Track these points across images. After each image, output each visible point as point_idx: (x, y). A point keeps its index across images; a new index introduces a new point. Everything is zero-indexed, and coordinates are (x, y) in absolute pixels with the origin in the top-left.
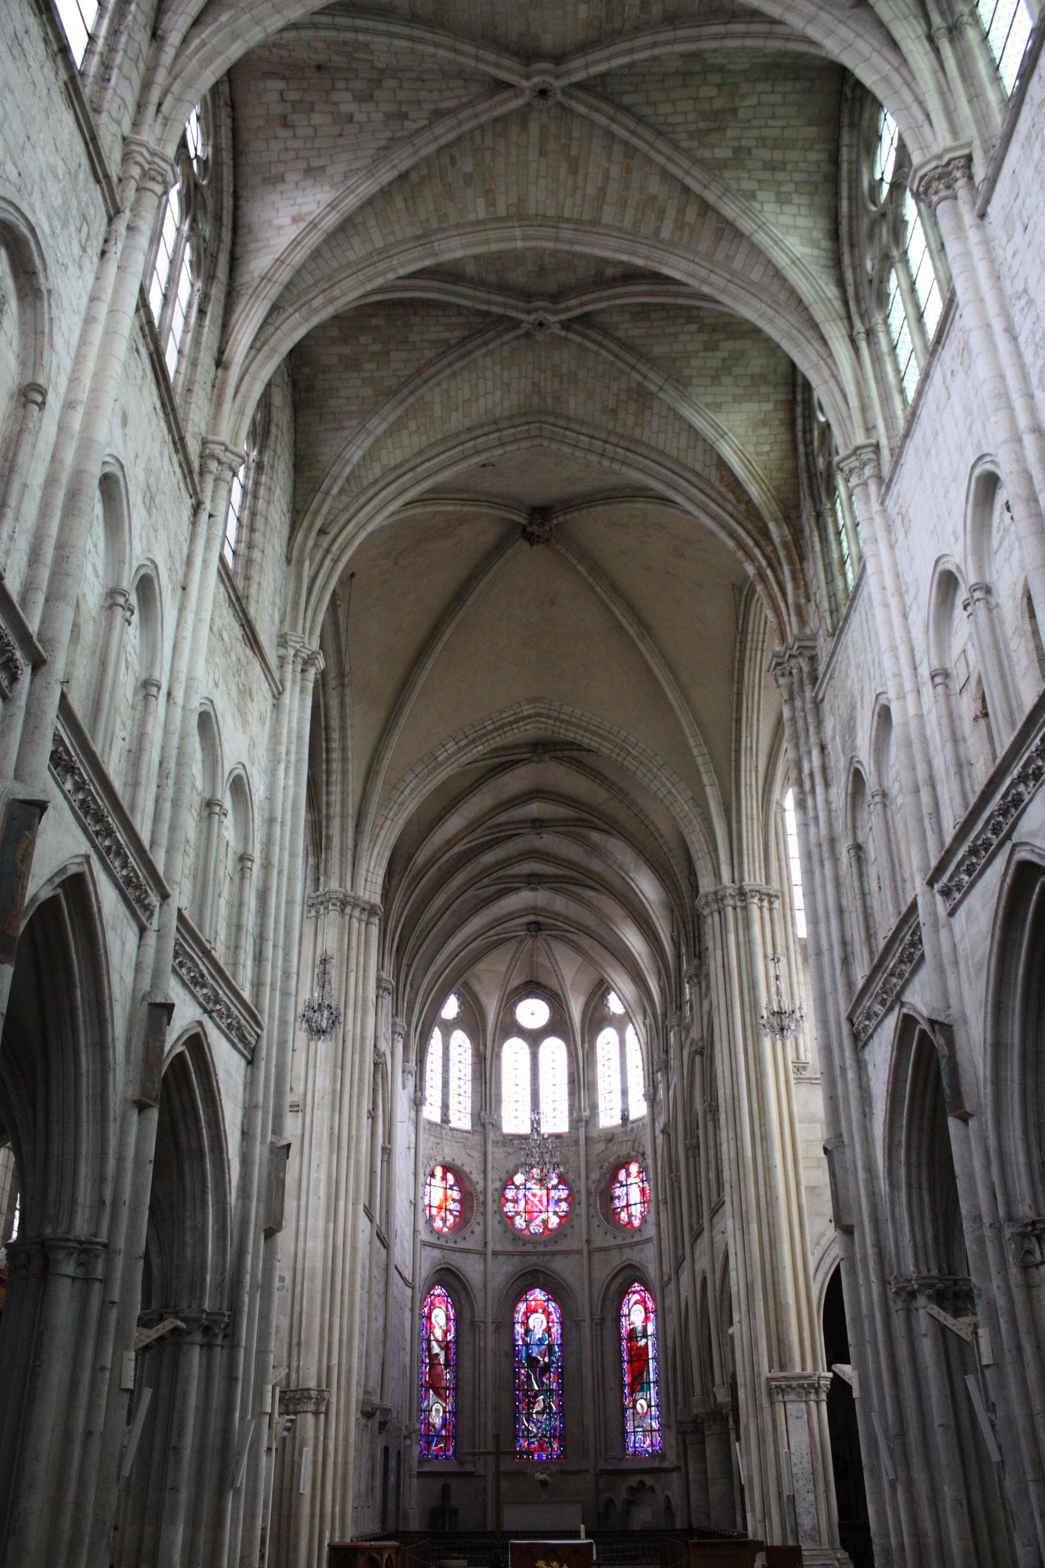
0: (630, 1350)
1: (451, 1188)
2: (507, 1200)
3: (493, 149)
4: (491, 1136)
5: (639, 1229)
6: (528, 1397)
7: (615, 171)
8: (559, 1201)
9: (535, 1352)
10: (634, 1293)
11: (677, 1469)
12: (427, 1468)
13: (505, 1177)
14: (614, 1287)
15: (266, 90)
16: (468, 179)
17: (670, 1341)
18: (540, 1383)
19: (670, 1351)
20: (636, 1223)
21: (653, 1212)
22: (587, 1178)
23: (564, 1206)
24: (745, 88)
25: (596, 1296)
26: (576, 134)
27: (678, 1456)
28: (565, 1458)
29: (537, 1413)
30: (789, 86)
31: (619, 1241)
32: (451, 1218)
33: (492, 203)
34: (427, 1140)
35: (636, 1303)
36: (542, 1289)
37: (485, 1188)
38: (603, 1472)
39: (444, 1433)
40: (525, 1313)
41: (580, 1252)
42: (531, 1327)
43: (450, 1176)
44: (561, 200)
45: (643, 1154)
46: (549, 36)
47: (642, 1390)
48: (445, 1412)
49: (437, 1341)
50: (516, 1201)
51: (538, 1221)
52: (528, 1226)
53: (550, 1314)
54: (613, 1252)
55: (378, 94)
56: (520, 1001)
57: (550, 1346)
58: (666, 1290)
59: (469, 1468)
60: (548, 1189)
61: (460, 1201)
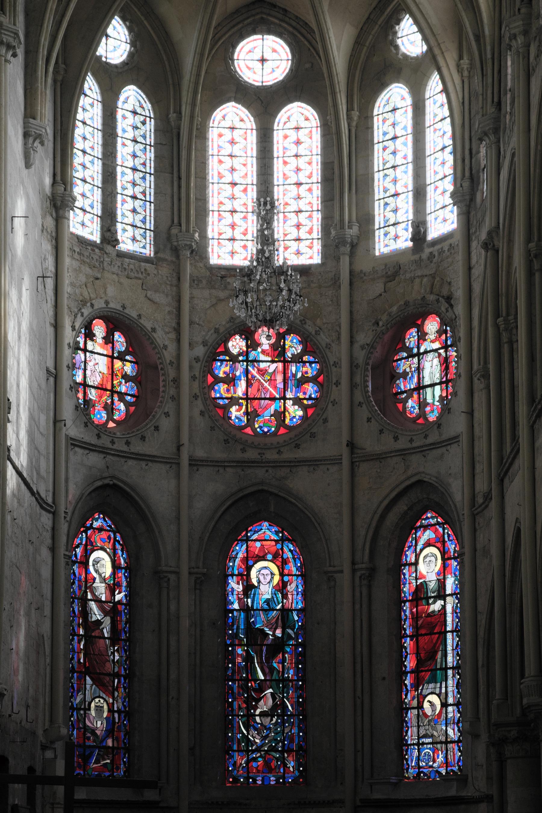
0: (416, 617)
1: (121, 357)
2: (218, 380)
4: (188, 269)
5: (438, 424)
6: (248, 690)
8: (304, 380)
10: (426, 527)
13: (211, 337)
14: (392, 518)
17: (483, 604)
18: (269, 670)
19: (482, 620)
20: (432, 417)
22: (352, 342)
23: (311, 389)
31: (402, 443)
32: (122, 407)
34: (78, 271)
36: (272, 522)
37: (178, 357)
39: (110, 743)
41: (337, 461)
42: (254, 581)
43: (117, 336)
47: (434, 680)
48: (111, 710)
49: (98, 601)
50: (231, 380)
51: (267, 415)
52: (250, 423)
53: (285, 562)
56: (242, 37)
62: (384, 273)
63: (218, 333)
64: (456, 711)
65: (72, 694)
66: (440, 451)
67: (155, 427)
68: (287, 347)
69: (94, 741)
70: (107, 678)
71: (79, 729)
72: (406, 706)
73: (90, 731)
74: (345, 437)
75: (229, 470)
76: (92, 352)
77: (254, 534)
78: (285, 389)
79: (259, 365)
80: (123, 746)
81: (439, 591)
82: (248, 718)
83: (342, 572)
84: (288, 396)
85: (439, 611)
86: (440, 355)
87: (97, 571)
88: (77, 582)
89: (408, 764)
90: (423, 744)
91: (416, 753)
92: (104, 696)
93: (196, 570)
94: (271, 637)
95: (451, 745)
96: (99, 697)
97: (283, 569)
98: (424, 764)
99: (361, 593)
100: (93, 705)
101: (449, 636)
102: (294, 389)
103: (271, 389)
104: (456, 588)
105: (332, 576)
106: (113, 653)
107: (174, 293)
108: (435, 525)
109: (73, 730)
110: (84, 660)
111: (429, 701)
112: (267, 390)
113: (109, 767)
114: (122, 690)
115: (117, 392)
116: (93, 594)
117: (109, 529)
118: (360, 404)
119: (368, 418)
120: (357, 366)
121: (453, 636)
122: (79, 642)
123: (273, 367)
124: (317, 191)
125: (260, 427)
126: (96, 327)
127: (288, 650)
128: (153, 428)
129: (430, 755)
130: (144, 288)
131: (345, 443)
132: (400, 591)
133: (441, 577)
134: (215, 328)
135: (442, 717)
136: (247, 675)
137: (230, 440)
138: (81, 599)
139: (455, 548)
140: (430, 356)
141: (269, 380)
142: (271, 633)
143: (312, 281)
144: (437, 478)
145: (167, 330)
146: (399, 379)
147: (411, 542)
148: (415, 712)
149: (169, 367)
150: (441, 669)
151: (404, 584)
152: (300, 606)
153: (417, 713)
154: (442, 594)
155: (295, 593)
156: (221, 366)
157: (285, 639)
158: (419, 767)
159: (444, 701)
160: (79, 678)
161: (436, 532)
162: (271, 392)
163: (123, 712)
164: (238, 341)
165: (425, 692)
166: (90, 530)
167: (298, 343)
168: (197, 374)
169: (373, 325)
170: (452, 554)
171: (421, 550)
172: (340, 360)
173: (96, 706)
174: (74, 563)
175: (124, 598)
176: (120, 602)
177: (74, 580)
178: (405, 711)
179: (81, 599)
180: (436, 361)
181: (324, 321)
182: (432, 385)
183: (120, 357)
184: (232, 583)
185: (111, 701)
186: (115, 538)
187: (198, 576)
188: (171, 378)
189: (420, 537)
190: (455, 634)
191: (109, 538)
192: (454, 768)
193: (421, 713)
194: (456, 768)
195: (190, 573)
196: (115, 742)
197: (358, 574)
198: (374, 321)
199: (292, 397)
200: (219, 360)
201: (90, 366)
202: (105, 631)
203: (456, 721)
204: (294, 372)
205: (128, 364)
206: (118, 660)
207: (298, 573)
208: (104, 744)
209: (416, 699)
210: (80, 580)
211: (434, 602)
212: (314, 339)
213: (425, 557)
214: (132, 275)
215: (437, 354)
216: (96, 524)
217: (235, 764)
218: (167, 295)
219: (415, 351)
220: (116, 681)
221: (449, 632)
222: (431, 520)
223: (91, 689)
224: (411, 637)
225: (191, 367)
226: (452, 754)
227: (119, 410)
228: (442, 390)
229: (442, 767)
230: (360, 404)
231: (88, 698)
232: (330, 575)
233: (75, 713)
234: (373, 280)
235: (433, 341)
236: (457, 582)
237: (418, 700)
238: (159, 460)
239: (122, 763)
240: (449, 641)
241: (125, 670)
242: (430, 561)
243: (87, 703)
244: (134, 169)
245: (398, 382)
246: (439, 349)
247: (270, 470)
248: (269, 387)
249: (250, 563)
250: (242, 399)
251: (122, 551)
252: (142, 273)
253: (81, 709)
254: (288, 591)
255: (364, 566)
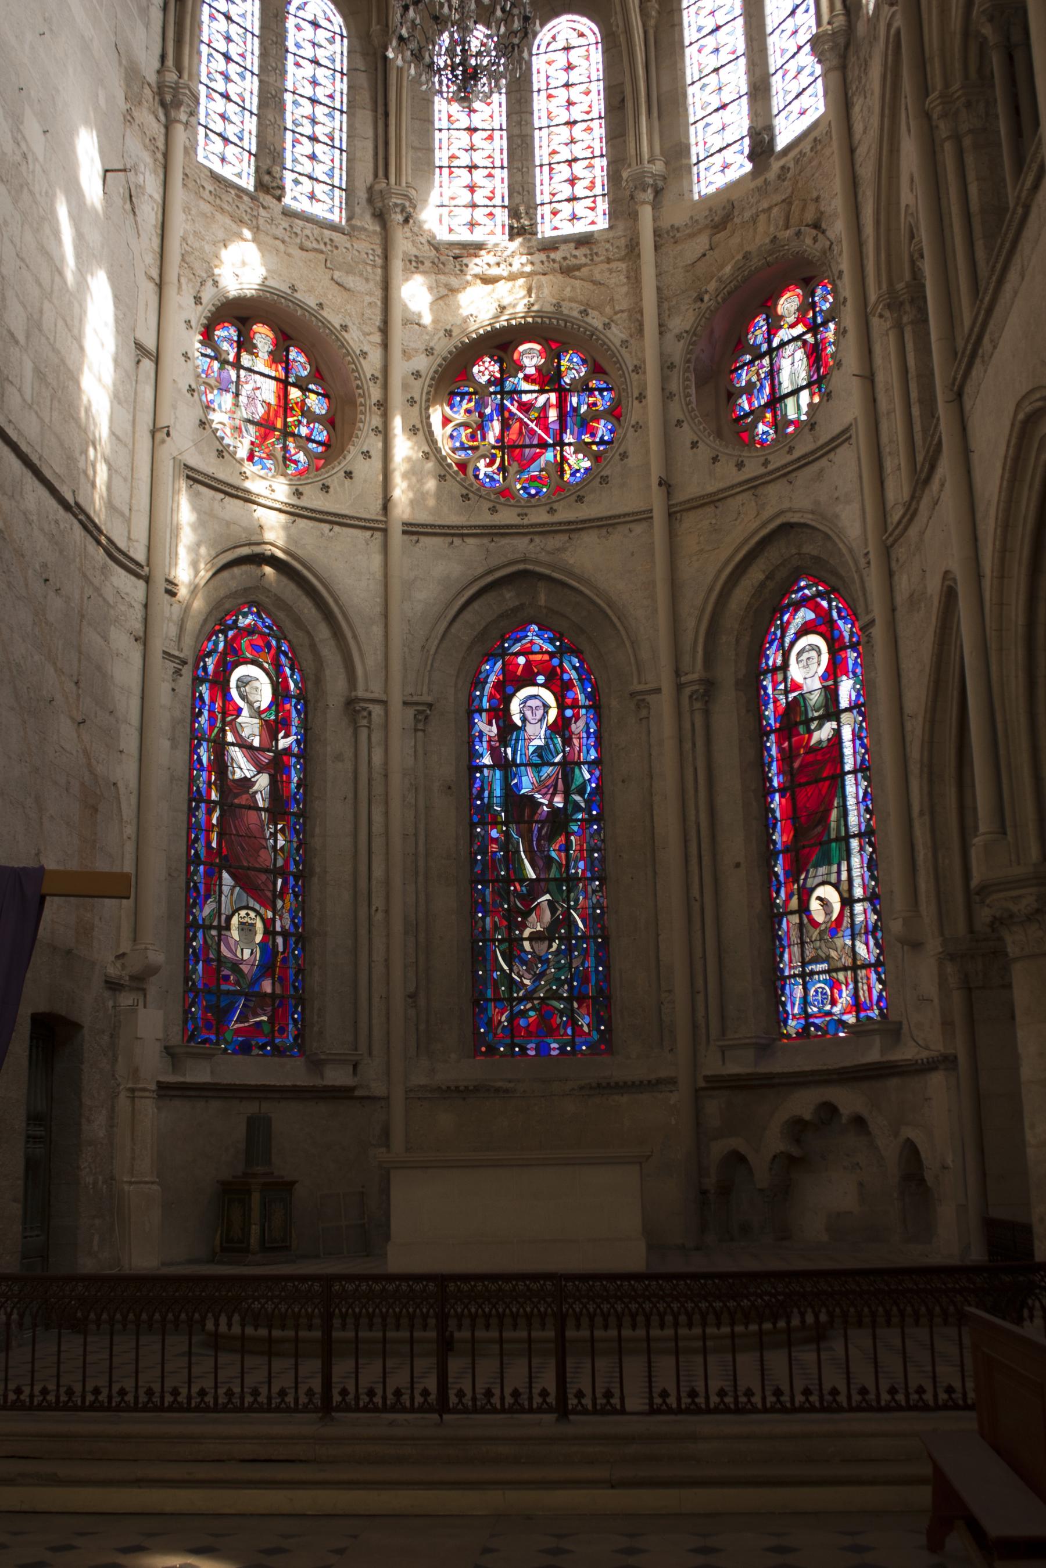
0: (786, 758)
4: (403, 244)
9: (527, 782)
10: (797, 606)
11: (947, 1062)
12: (199, 1074)
14: (741, 595)
18: (542, 862)
21: (851, 338)
22: (662, 329)
23: (602, 429)
25: (690, 623)
27: (947, 1024)
28: (610, 1050)
29: (534, 938)
31: (753, 470)
32: (301, 457)
35: (806, 629)
38: (718, 1083)
39: (267, 986)
40: (498, 686)
41: (644, 517)
42: (517, 719)
45: (816, 226)
48: (269, 931)
49: (245, 746)
54: (734, 503)
57: (568, 767)
58: (900, 552)
59: (337, 1076)
60: (563, 394)
61: (330, 421)
62: (708, 222)
63: (450, 336)
64: (869, 911)
65: (195, 901)
66: (815, 467)
67: (345, 472)
68: (563, 369)
69: (237, 983)
70: (264, 877)
71: (207, 961)
72: (778, 910)
73: (229, 965)
74: (656, 471)
75: (470, 541)
76: (249, 370)
77: (514, 644)
78: (563, 428)
79: (520, 398)
80: (292, 992)
81: (826, 706)
82: (510, 945)
83: (658, 691)
84: (567, 441)
85: (828, 740)
86: (805, 342)
87: (243, 697)
88: (206, 713)
89: (786, 1012)
90: (812, 973)
91: (799, 992)
92: (257, 907)
93: (415, 699)
94: (545, 808)
95: (864, 972)
96: (247, 907)
97: (564, 696)
98: (815, 1009)
99: (693, 725)
100: (235, 921)
101: (850, 780)
102: (576, 429)
103: (540, 432)
104: (858, 696)
105: (643, 700)
106: (274, 835)
107: (378, 278)
108: (813, 597)
109: (197, 963)
110: (219, 843)
111: (819, 898)
112: (532, 432)
113: (266, 1029)
114: (290, 897)
115: (293, 434)
116: (236, 733)
117: (267, 631)
118: (679, 423)
119: (692, 443)
120: (672, 366)
121: (856, 779)
122: (209, 813)
123: (542, 399)
124: (599, 130)
125: (524, 488)
126: (257, 336)
127: (575, 828)
128: (342, 474)
129: (826, 994)
130: (328, 265)
131: (654, 481)
132: (761, 717)
133: (831, 683)
134: (446, 330)
135: (845, 924)
136: (507, 870)
137: (471, 495)
138: (214, 741)
139: (851, 628)
140: (790, 348)
141: (536, 418)
142: (546, 802)
143: (596, 254)
144: (813, 512)
145: (367, 330)
146: (741, 397)
147: (775, 634)
148: (795, 919)
149: (371, 384)
150: (838, 839)
151: (766, 705)
152: (593, 754)
153: (798, 921)
154: (832, 710)
155: (584, 735)
156: (461, 401)
157: (569, 812)
158: (807, 1016)
159: (846, 895)
160: (208, 874)
161: (816, 608)
162: (540, 436)
163: (293, 935)
164: (487, 364)
165: (810, 883)
166: (231, 629)
167: (580, 363)
168: (417, 398)
169: (695, 301)
170: (847, 639)
171: (793, 643)
172: (644, 362)
173: (241, 923)
174: (202, 681)
175: (294, 745)
176: (287, 751)
177: (200, 710)
178: (776, 920)
179: (214, 741)
180: (800, 354)
181: (617, 308)
182: (796, 392)
183: (299, 383)
184: (480, 724)
185: (270, 915)
186: (279, 647)
187: (420, 708)
188: (374, 400)
189: (789, 622)
190: (860, 775)
191: (269, 646)
192: (870, 1014)
193: (806, 920)
194: (874, 1013)
195: (405, 703)
196: (278, 985)
197: (687, 691)
198: (695, 295)
199: (572, 440)
200: (458, 394)
201: (246, 389)
202: (258, 797)
203: (870, 928)
204: (575, 405)
205: (313, 396)
206: (282, 848)
207: (587, 703)
208: (256, 989)
209: (796, 897)
210: (211, 712)
211: (820, 727)
212: (602, 336)
213: (799, 654)
214: (308, 244)
215: (800, 343)
216: (244, 622)
217: (491, 1020)
218: (367, 280)
219: (765, 347)
220: (280, 881)
221: (849, 772)
222: (806, 591)
223: (232, 894)
224: (782, 790)
225: (405, 387)
226: (865, 987)
227: (296, 462)
228: (812, 395)
229: (850, 1012)
230: (679, 423)
231: (226, 909)
232: (639, 697)
233: (200, 935)
234: (692, 236)
235: (792, 326)
236: (858, 686)
237: (799, 899)
238: (352, 522)
239: (291, 1022)
240: (850, 789)
241: (297, 863)
242: (808, 658)
243: (223, 917)
244: (314, 101)
245: (740, 401)
246: (804, 334)
247: (537, 539)
248: (536, 429)
249: (509, 689)
250: (494, 447)
251: (292, 669)
252: (325, 244)
253: (211, 927)
254: (573, 733)
255: (695, 676)
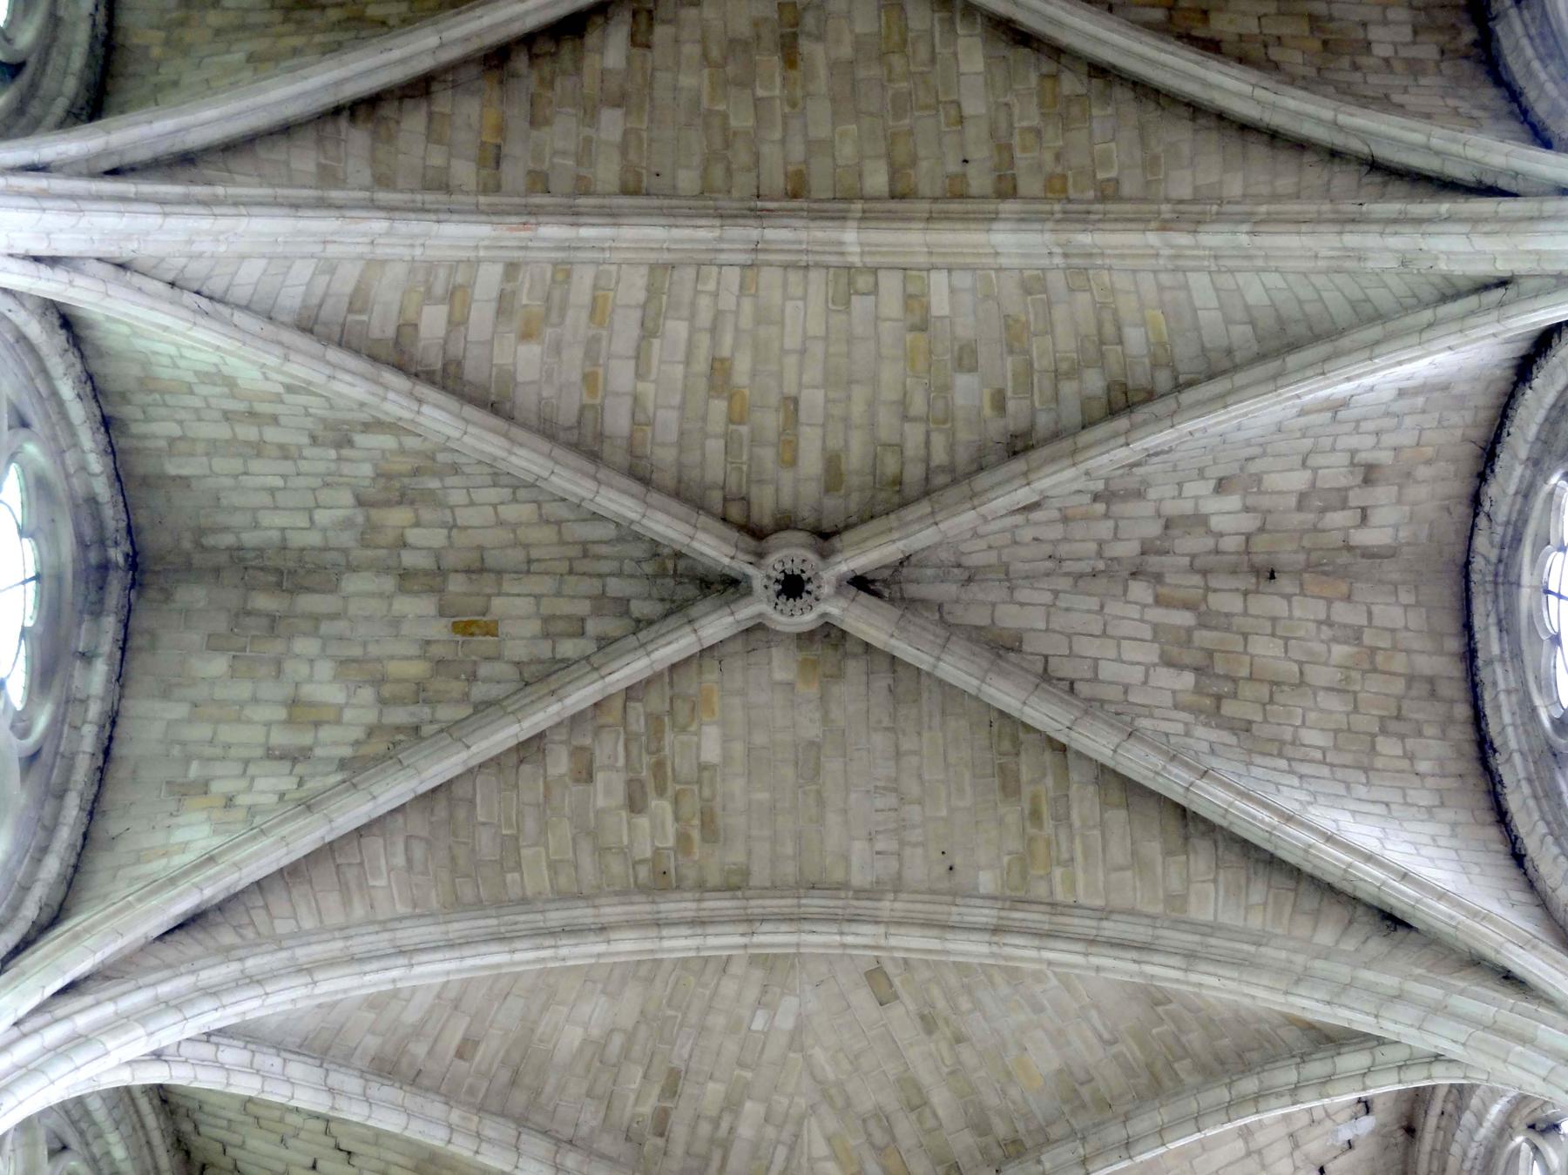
3: (905, 418)
7: (621, 375)
15: (1396, 527)
16: (966, 358)
24: (347, 539)
26: (715, 446)
30: (250, 538)
33: (915, 301)
44: (747, 305)
46: (779, 675)
55: (1153, 529)
